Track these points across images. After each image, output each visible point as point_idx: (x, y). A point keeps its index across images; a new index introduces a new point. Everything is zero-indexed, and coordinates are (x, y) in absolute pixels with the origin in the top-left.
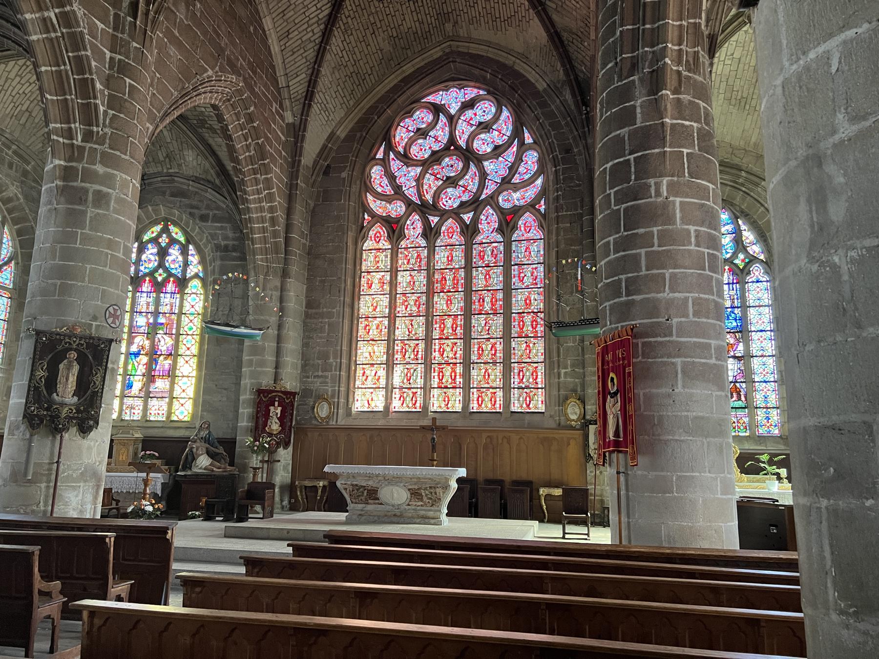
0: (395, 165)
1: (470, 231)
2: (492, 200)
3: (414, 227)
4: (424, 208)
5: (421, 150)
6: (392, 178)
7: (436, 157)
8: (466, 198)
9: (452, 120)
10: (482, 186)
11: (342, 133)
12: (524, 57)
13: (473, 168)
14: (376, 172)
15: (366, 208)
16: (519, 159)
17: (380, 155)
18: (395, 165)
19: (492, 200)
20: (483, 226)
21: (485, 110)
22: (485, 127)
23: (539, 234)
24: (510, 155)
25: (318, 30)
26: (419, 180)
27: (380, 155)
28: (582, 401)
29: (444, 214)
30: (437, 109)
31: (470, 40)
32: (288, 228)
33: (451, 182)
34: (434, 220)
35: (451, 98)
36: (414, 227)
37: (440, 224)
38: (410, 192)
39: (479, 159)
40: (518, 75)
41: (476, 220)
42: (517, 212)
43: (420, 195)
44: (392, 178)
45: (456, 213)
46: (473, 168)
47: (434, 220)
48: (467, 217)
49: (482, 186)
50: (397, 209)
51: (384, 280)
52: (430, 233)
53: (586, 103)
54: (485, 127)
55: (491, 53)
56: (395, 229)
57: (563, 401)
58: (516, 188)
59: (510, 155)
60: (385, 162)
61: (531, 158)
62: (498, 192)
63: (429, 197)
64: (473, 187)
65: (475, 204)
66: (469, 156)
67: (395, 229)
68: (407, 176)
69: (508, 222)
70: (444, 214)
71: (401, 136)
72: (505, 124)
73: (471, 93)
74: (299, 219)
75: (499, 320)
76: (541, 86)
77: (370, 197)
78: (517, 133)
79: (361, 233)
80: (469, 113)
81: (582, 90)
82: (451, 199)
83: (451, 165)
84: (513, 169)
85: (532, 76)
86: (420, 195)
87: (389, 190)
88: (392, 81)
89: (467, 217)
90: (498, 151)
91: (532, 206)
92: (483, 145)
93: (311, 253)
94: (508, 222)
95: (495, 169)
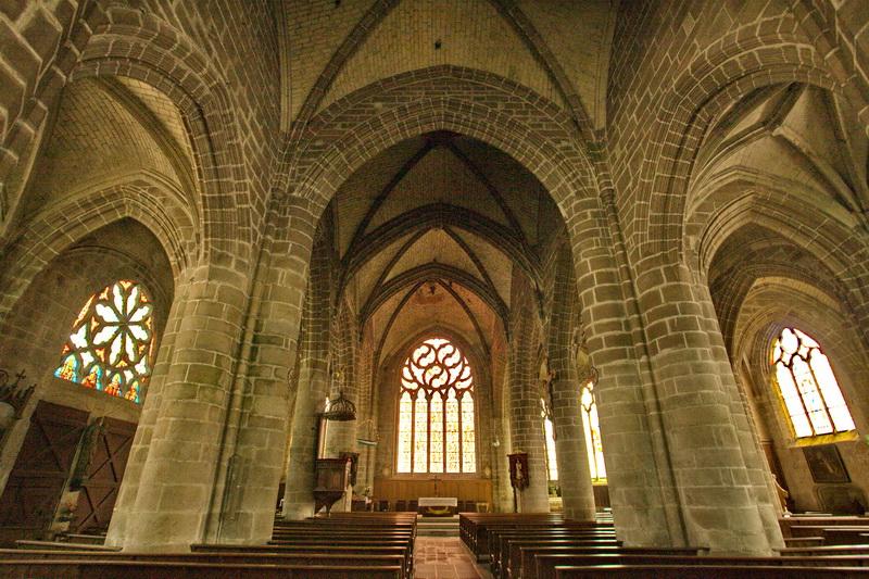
0: (414, 368)
1: (444, 397)
2: (453, 385)
3: (421, 393)
4: (427, 387)
5: (424, 362)
6: (412, 373)
7: (430, 366)
8: (443, 383)
9: (437, 352)
10: (449, 379)
11: (392, 354)
12: (465, 332)
13: (445, 372)
14: (406, 370)
15: (401, 384)
16: (463, 370)
17: (407, 363)
18: (414, 368)
19: (453, 385)
20: (449, 395)
21: (449, 349)
22: (449, 356)
23: (472, 400)
24: (460, 366)
25: (389, 317)
26: (424, 375)
27: (407, 363)
28: (491, 468)
29: (434, 390)
30: (430, 347)
31: (444, 322)
32: (373, 393)
33: (436, 376)
34: (430, 391)
35: (436, 343)
36: (421, 393)
37: (432, 393)
38: (421, 381)
39: (448, 368)
40: (463, 338)
41: (447, 392)
42: (463, 390)
43: (424, 381)
44: (412, 373)
45: (439, 389)
46: (445, 372)
47: (430, 391)
48: (443, 391)
49: (449, 379)
50: (414, 386)
51: (410, 414)
52: (429, 397)
53: (489, 353)
54: (449, 356)
55: (453, 328)
56: (414, 395)
57: (483, 468)
58: (462, 381)
59: (460, 366)
60: (409, 366)
61: (467, 369)
62: (456, 381)
63: (428, 382)
64: (445, 380)
65: (446, 386)
66: (443, 366)
67: (414, 395)
68: (418, 373)
69: (459, 394)
70: (434, 390)
71: (417, 354)
72: (457, 357)
73: (443, 341)
74: (376, 390)
75: (457, 434)
76: (472, 343)
77: (403, 381)
78: (462, 359)
79: (400, 396)
80: (442, 350)
81: (487, 348)
82: (436, 383)
83: (436, 370)
84: (461, 373)
85: (468, 339)
86: (424, 381)
87: (410, 378)
88: (412, 335)
89: (443, 391)
90: (455, 366)
91: (468, 389)
92: (449, 362)
93: (380, 404)
94: (459, 394)
95: (455, 373)
